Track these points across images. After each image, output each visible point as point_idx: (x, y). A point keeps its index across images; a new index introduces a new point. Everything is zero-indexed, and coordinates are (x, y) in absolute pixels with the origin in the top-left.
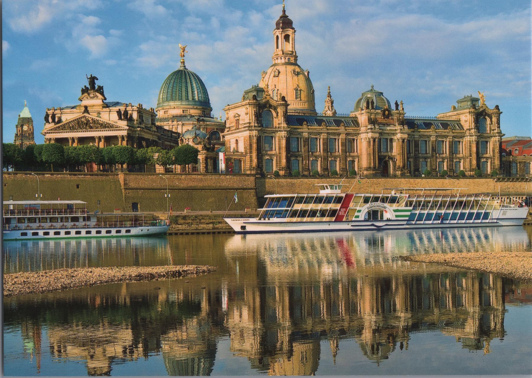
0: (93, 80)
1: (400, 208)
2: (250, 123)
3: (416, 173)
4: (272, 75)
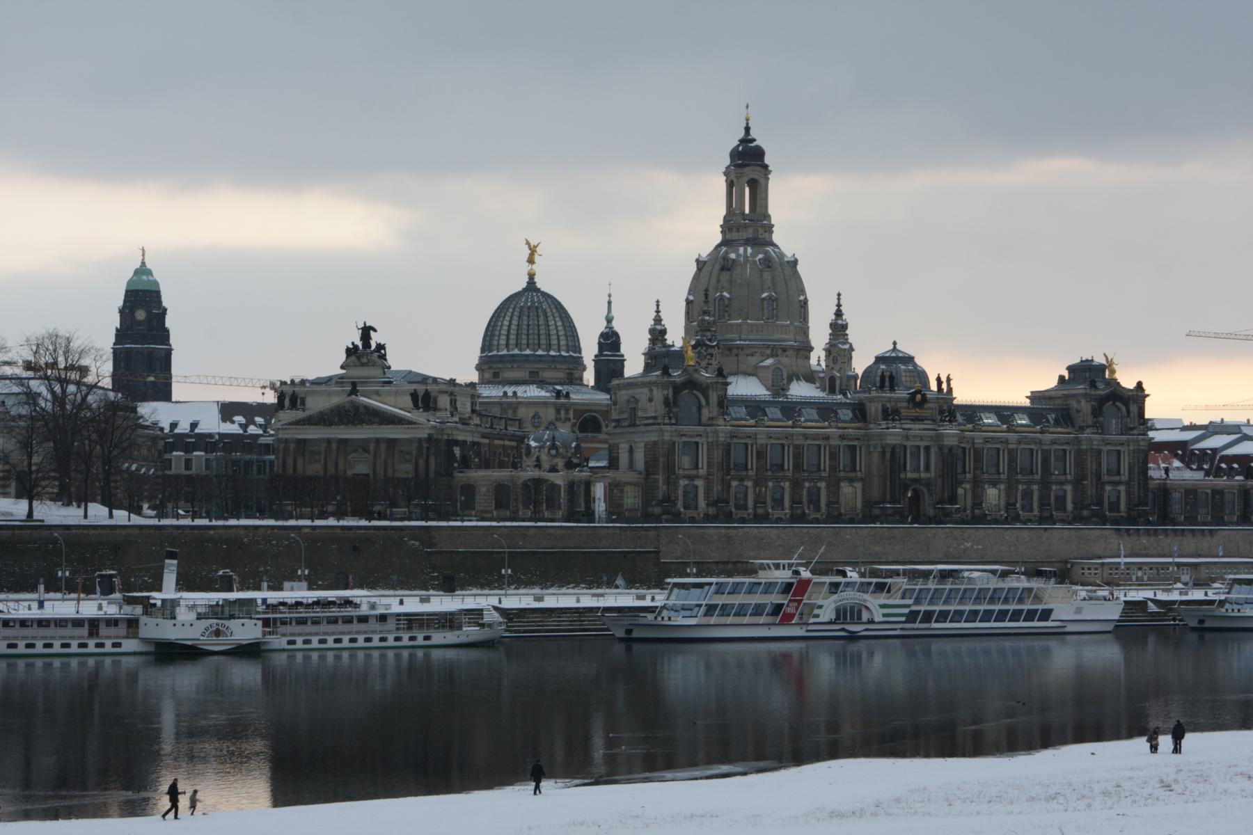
0: (366, 332)
1: (891, 602)
2: (655, 418)
3: (977, 511)
4: (717, 267)
